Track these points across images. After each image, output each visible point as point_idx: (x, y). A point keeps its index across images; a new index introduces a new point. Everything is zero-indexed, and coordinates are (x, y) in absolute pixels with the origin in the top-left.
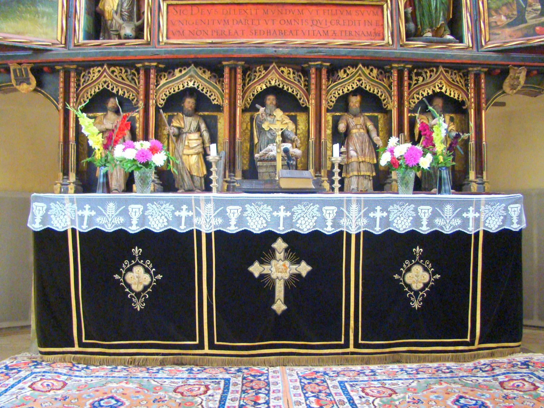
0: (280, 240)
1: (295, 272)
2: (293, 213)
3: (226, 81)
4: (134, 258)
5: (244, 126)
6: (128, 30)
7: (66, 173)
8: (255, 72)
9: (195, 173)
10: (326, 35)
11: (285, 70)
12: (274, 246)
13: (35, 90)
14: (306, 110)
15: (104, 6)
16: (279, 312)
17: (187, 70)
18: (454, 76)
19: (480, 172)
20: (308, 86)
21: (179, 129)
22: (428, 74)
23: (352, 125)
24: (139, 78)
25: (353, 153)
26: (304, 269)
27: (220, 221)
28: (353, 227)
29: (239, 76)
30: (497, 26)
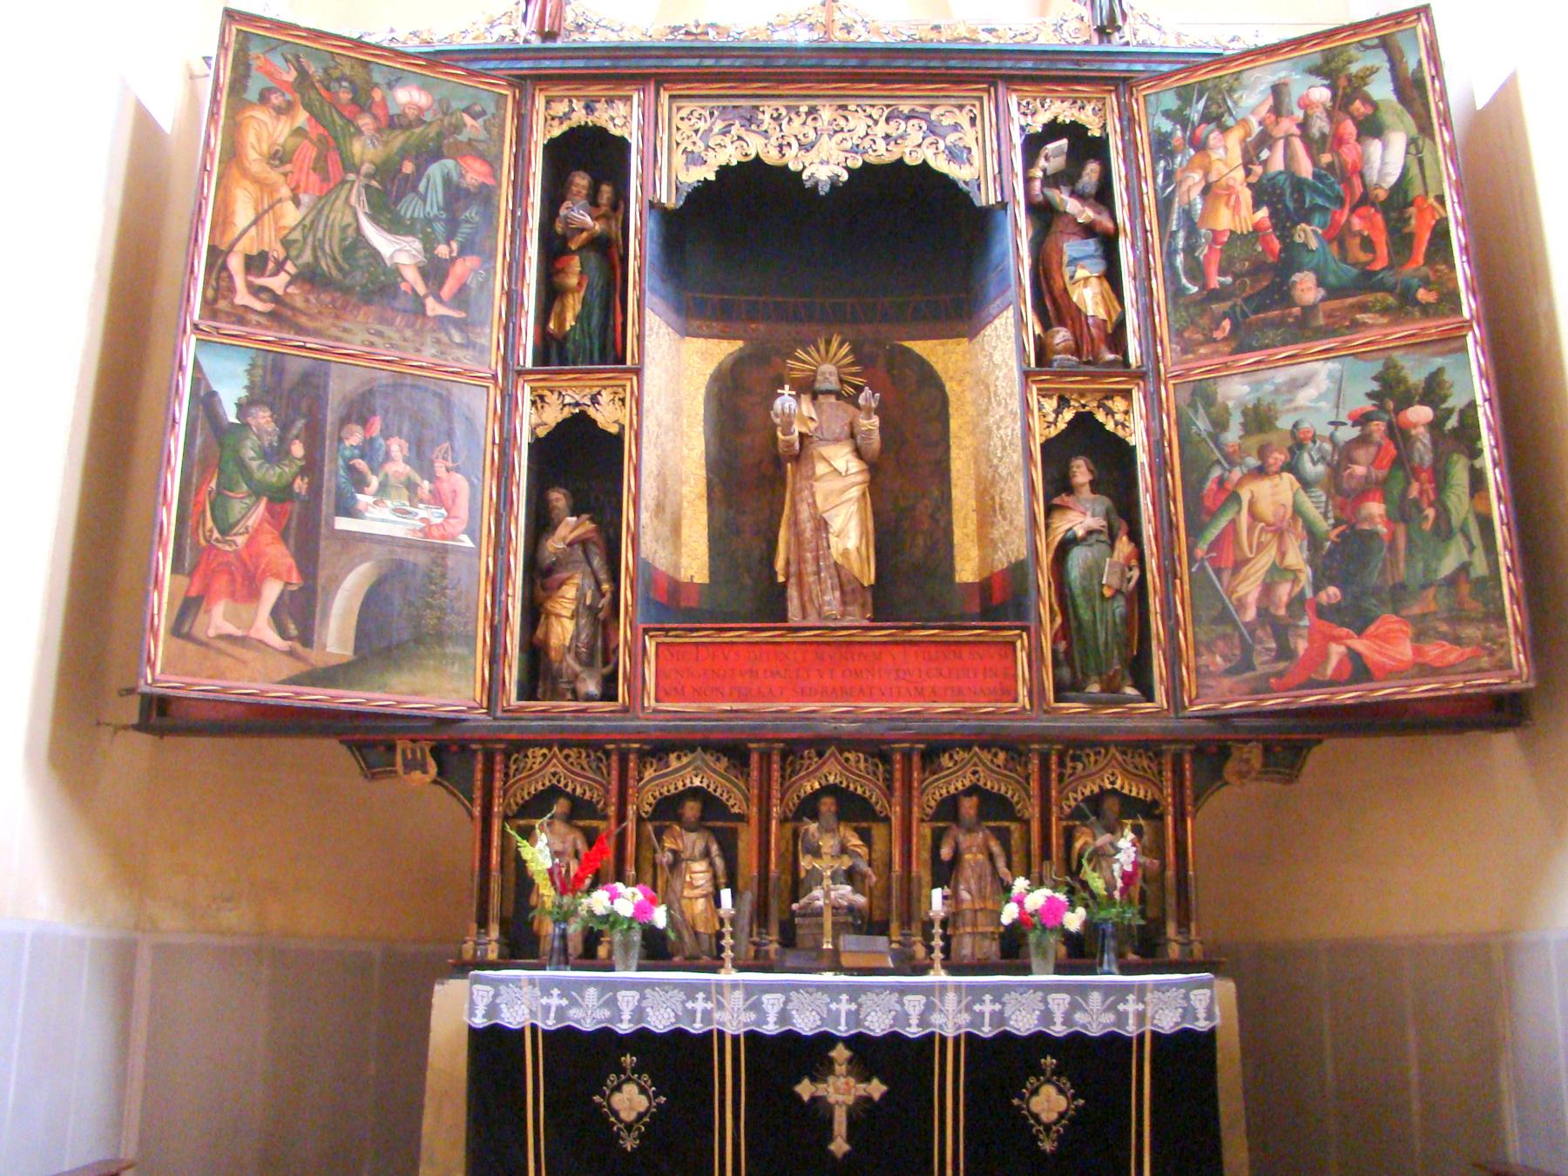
0: (840, 1047)
1: (862, 1093)
2: (860, 1005)
3: (755, 774)
4: (624, 1071)
5: (783, 844)
6: (591, 686)
7: (483, 922)
8: (802, 757)
9: (701, 929)
10: (920, 695)
11: (851, 756)
12: (833, 1054)
13: (435, 782)
14: (887, 819)
15: (547, 634)
16: (839, 1154)
17: (690, 756)
18: (1137, 760)
19: (1183, 923)
20: (889, 781)
21: (675, 853)
22: (1092, 759)
23: (963, 846)
24: (609, 766)
25: (965, 895)
26: (876, 1088)
27: (753, 1016)
28: (950, 1025)
29: (775, 766)
30: (1211, 675)
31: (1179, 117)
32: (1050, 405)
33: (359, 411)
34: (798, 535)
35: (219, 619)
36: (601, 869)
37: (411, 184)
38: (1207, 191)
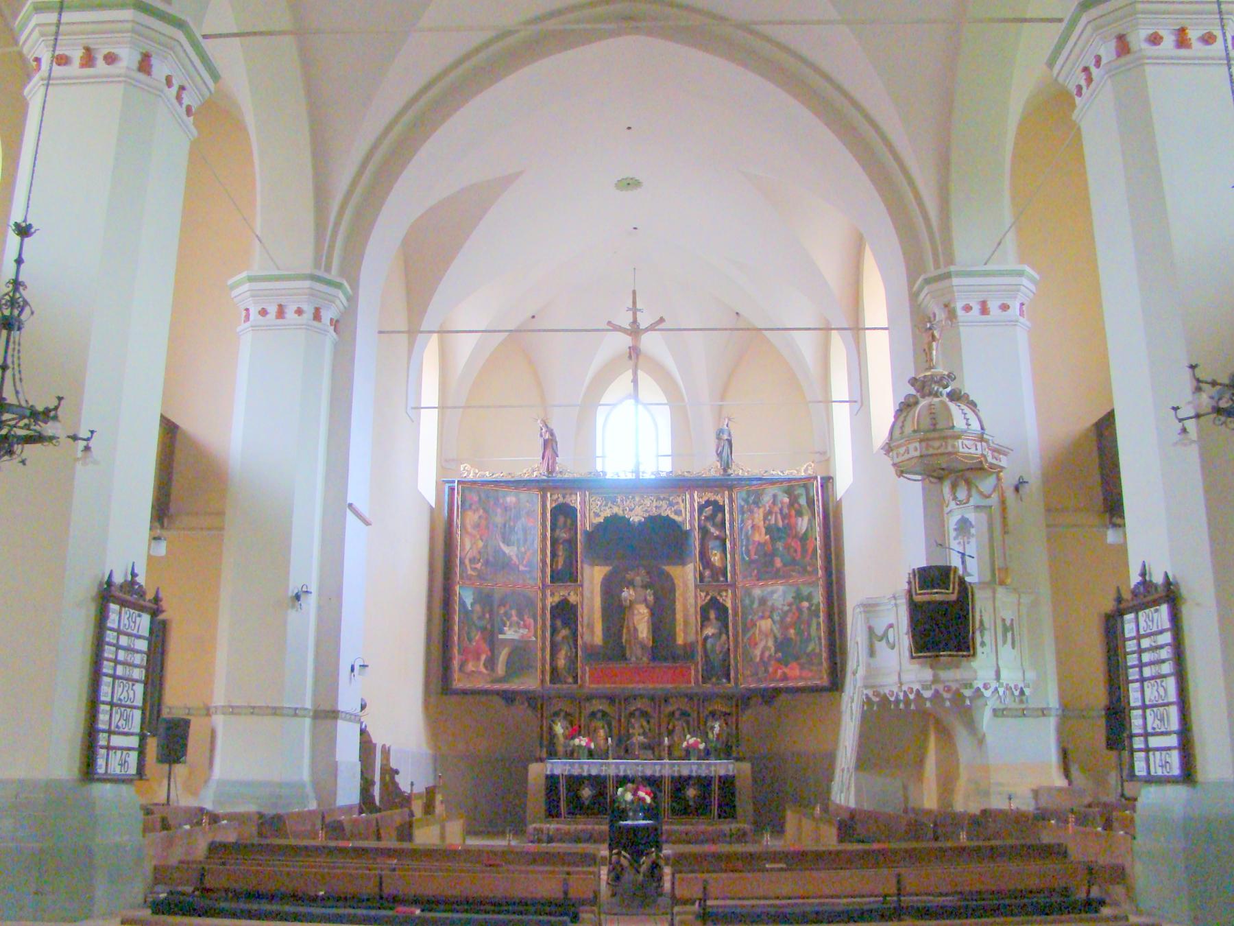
6: (570, 680)
31: (746, 501)
32: (703, 594)
33: (502, 603)
34: (629, 631)
35: (470, 667)
36: (575, 732)
37: (512, 529)
38: (753, 526)
